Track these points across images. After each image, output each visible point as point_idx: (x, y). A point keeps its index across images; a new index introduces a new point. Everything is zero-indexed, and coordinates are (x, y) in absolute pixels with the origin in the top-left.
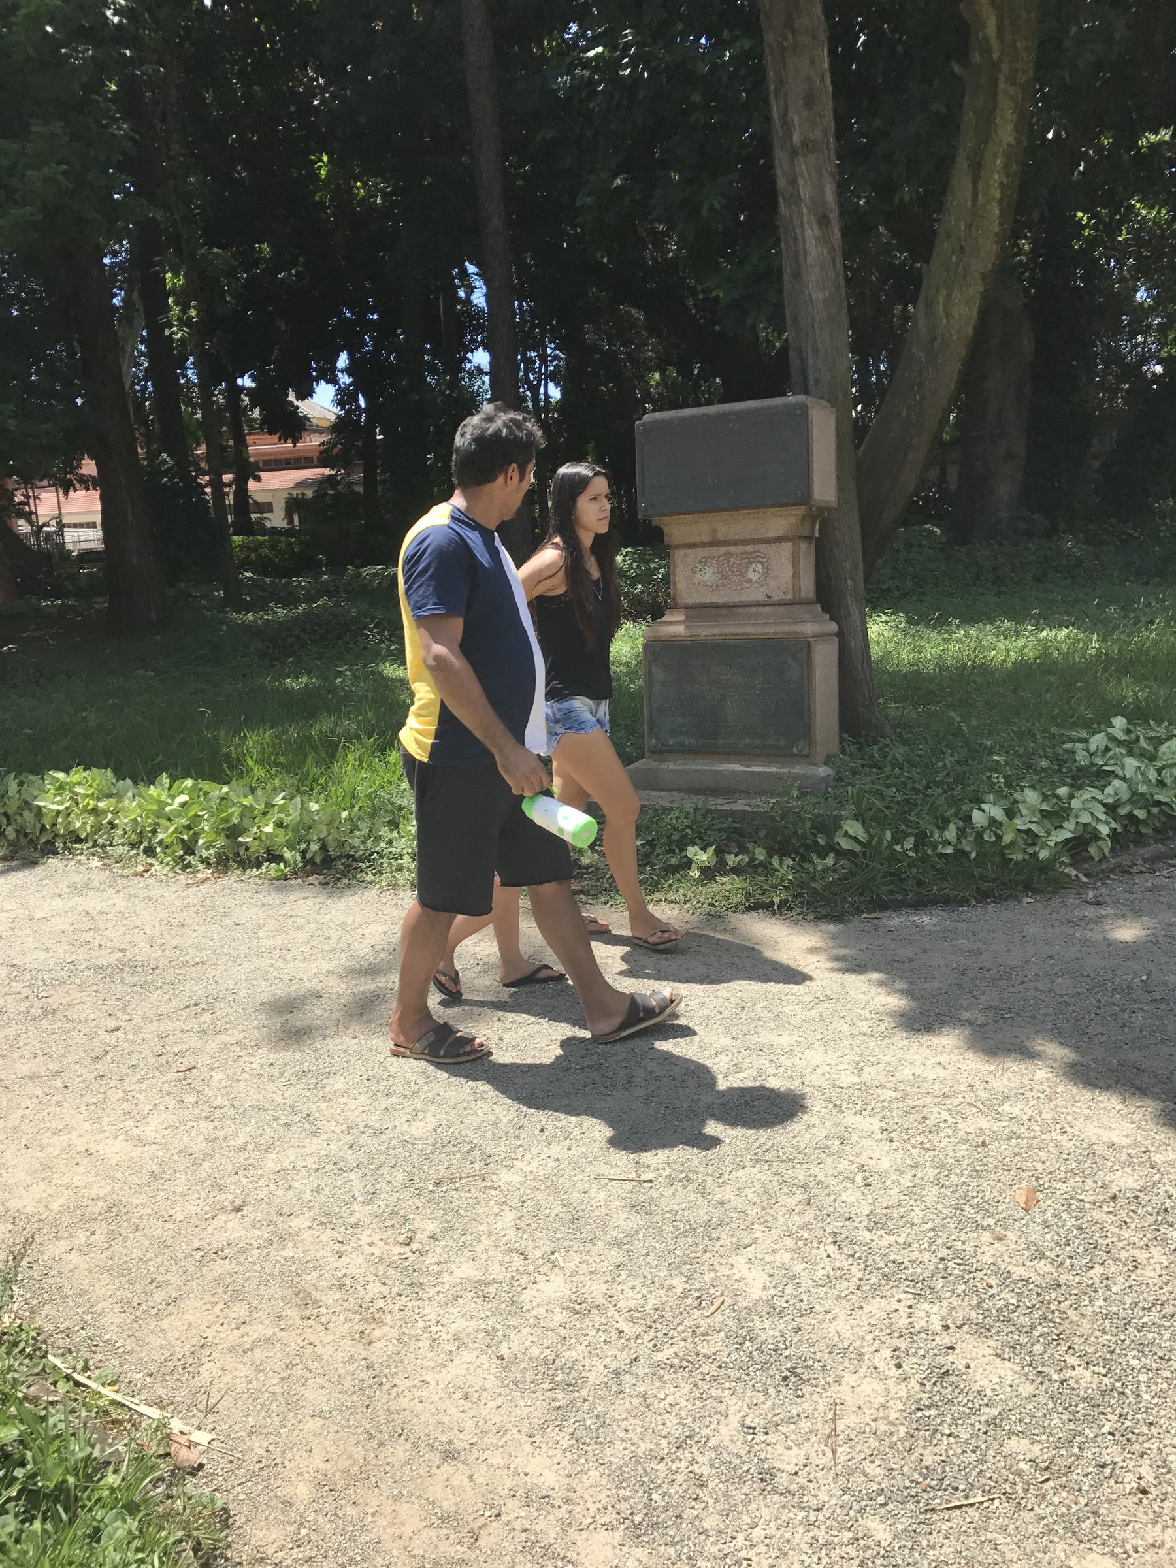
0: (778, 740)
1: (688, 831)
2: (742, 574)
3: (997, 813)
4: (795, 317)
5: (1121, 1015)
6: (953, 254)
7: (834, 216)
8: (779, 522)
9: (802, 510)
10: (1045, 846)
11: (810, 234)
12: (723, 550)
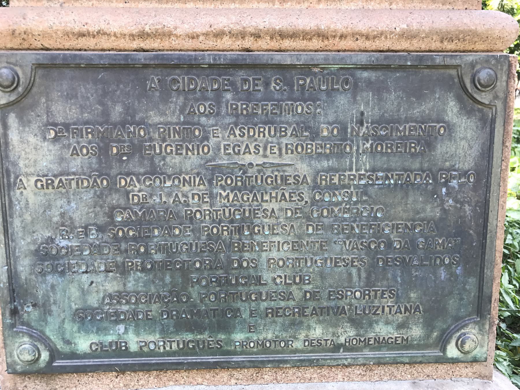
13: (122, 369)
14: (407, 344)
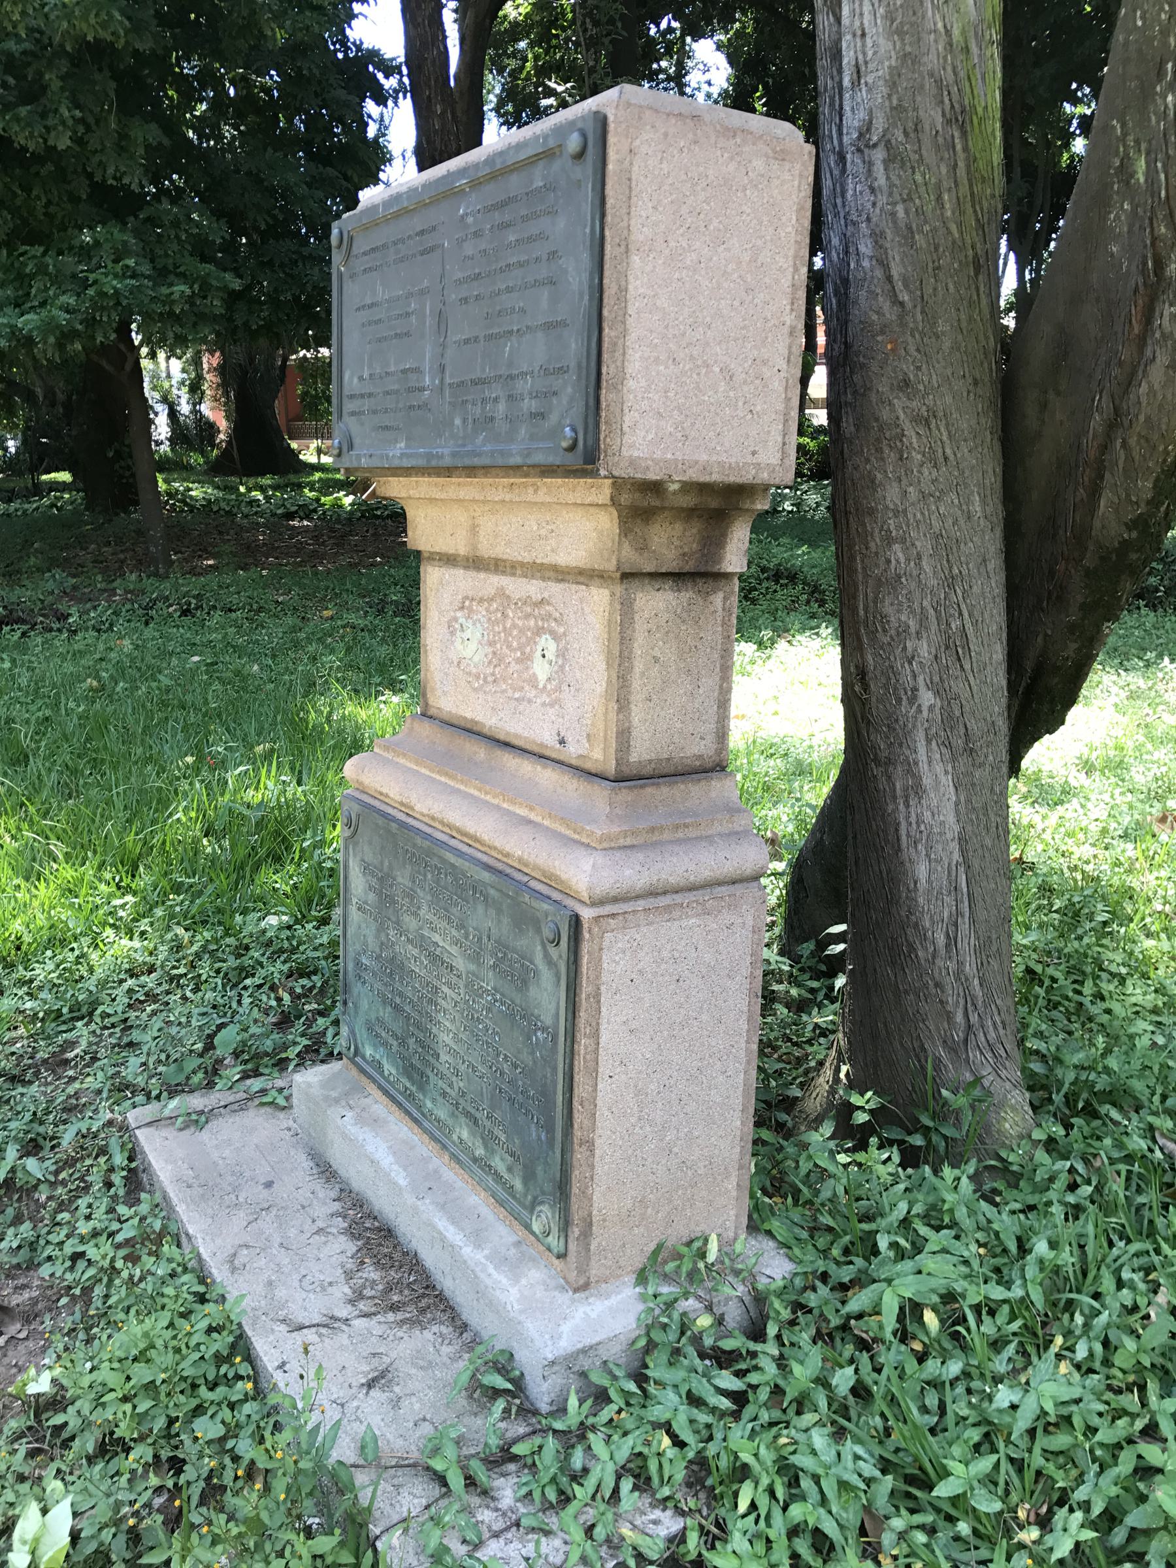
2: (526, 659)
12: (495, 581)
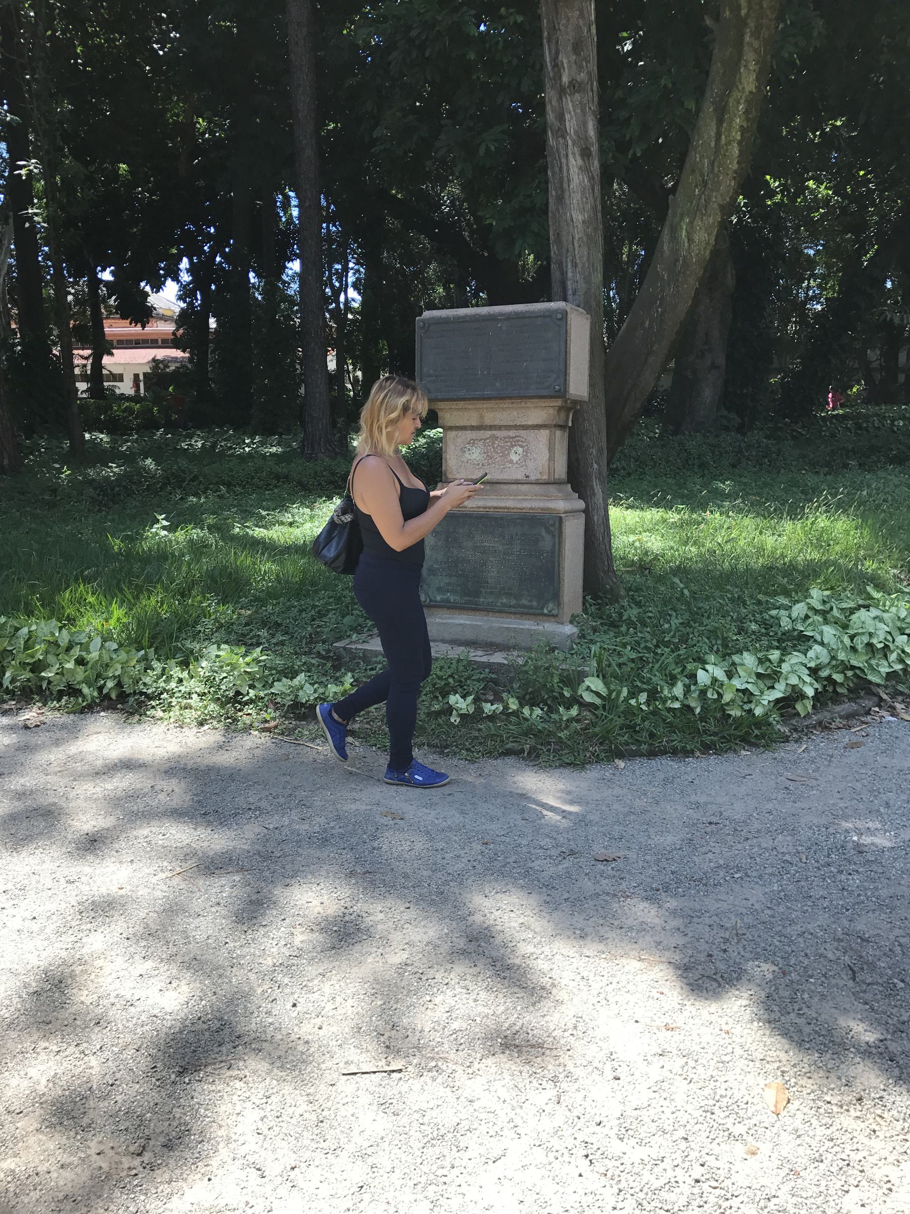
0: (530, 601)
1: (451, 680)
2: (505, 455)
3: (720, 674)
4: (558, 234)
5: (839, 877)
6: (696, 186)
7: (594, 149)
8: (539, 413)
9: (559, 403)
10: (758, 703)
11: (574, 163)
12: (489, 433)
13: (449, 608)
14: (531, 607)
